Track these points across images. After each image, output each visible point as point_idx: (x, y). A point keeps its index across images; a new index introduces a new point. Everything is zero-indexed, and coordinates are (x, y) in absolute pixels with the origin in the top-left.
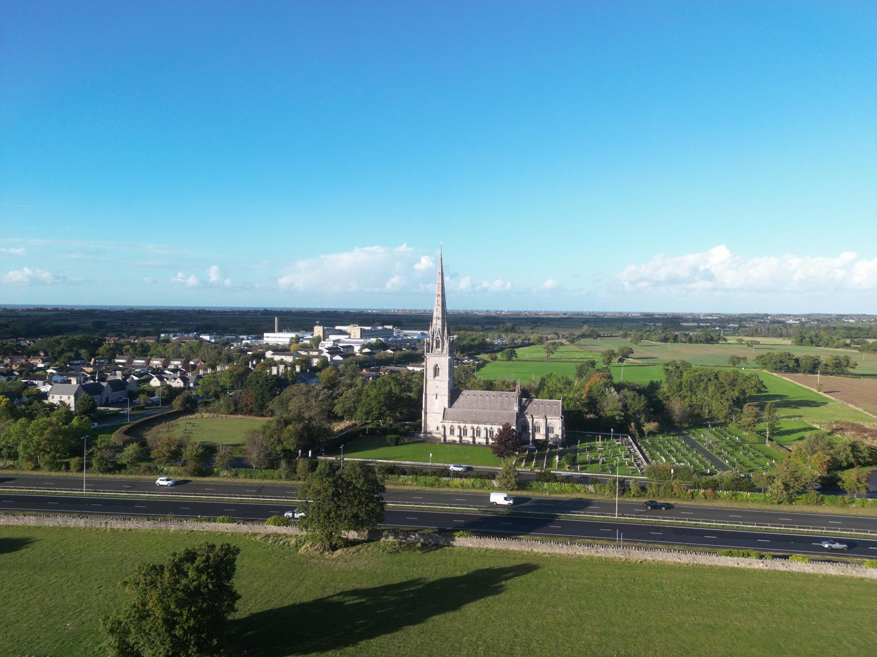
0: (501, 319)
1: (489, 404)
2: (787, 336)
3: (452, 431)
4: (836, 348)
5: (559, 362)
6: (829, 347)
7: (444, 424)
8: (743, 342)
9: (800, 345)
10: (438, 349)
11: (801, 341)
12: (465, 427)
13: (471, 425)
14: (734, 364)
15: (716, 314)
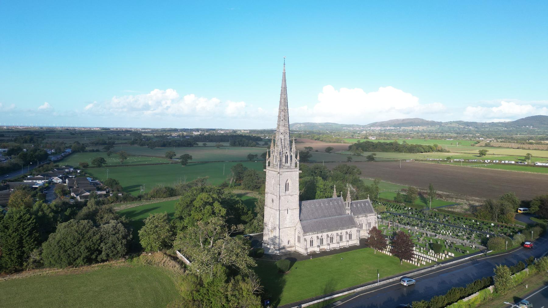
0: (319, 134)
1: (327, 211)
2: (215, 142)
3: (312, 242)
4: (252, 147)
5: (126, 166)
6: (248, 147)
7: (305, 237)
8: (206, 146)
9: (234, 146)
10: (287, 165)
11: (234, 144)
12: (322, 236)
13: (326, 233)
14: (251, 159)
15: (150, 129)
